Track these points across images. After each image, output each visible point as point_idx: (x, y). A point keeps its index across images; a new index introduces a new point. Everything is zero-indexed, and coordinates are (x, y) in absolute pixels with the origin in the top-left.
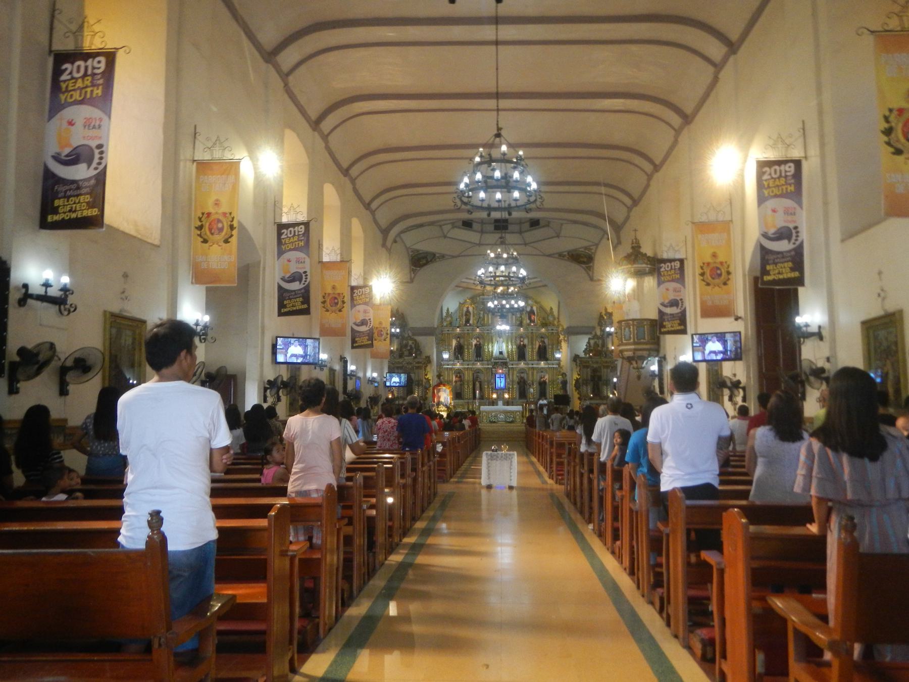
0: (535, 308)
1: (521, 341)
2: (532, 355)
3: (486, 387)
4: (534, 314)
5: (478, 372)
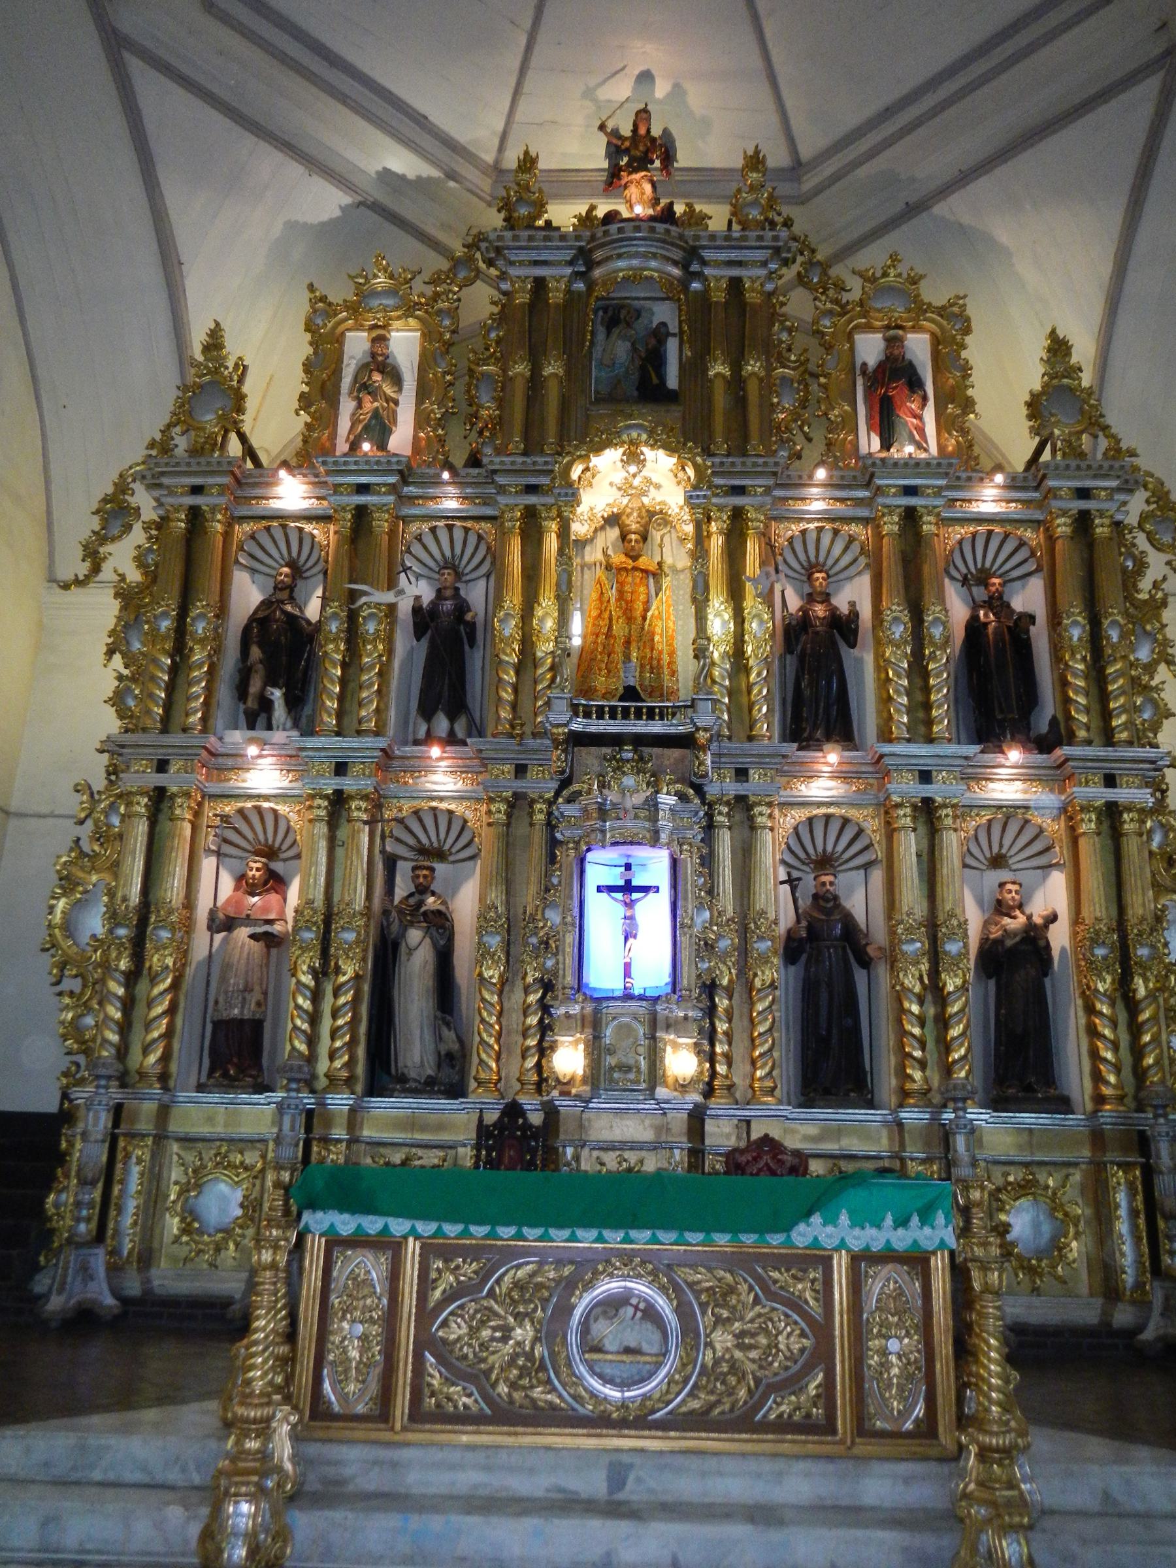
1: (810, 598)
2: (922, 707)
4: (915, 383)
5: (440, 855)
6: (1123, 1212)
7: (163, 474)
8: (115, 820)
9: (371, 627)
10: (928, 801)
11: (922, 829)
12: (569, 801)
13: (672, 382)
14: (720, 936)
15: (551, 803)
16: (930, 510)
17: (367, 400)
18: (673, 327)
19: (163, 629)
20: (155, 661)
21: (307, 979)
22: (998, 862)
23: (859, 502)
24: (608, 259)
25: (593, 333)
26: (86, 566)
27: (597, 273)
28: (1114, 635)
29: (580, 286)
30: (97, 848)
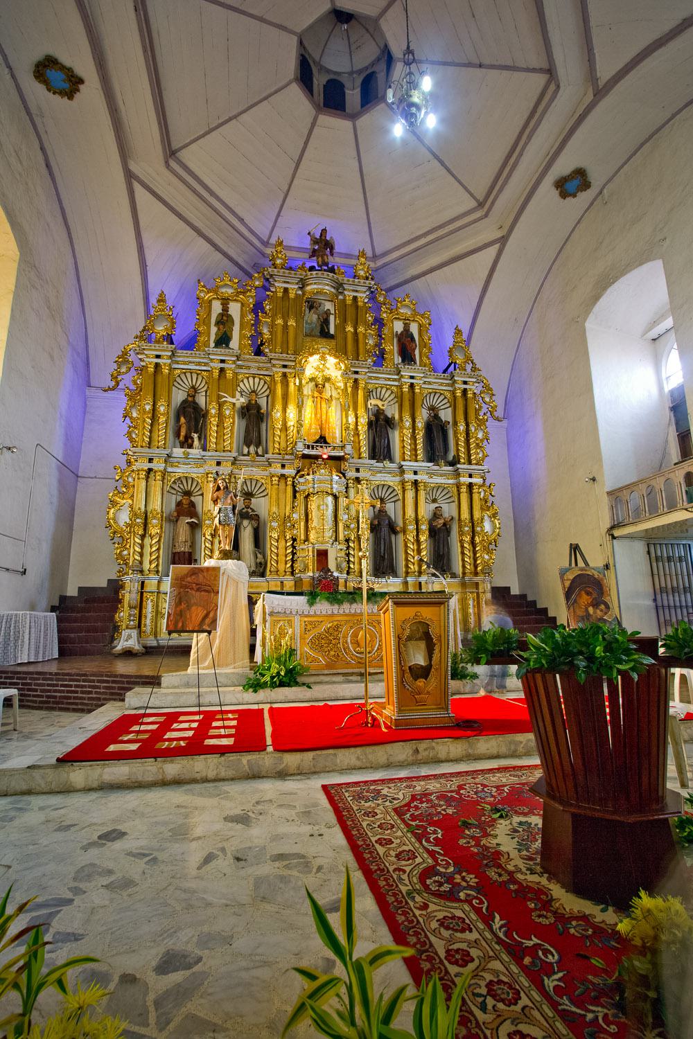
0: (414, 329)
3: (275, 535)
6: (471, 606)
7: (144, 349)
8: (130, 479)
9: (227, 412)
10: (416, 481)
11: (414, 490)
12: (300, 477)
13: (332, 331)
14: (351, 523)
15: (294, 478)
16: (418, 385)
17: (221, 327)
18: (333, 312)
19: (147, 410)
20: (144, 421)
21: (209, 538)
22: (434, 501)
23: (395, 380)
24: (311, 284)
25: (305, 310)
26: (113, 383)
27: (308, 288)
28: (473, 429)
29: (300, 292)
30: (125, 491)
